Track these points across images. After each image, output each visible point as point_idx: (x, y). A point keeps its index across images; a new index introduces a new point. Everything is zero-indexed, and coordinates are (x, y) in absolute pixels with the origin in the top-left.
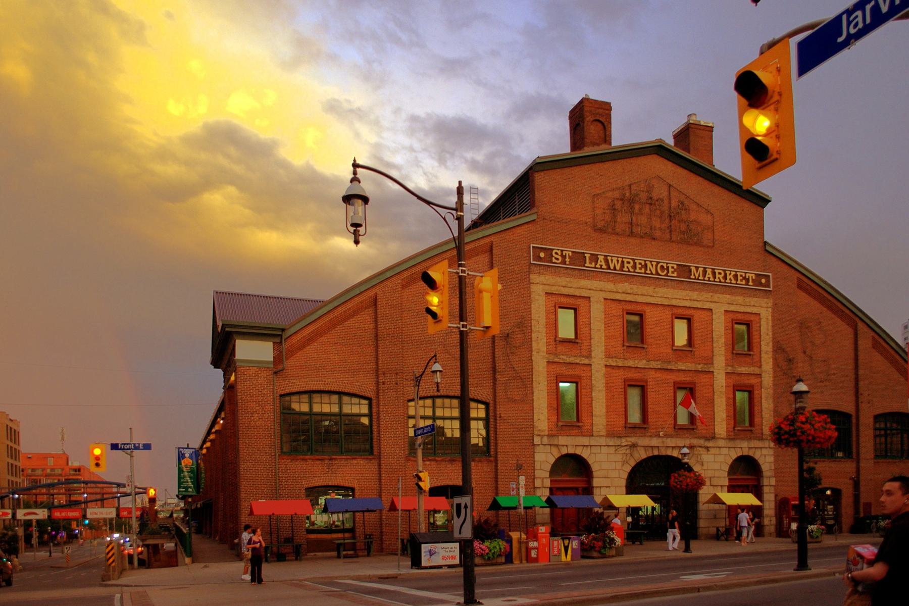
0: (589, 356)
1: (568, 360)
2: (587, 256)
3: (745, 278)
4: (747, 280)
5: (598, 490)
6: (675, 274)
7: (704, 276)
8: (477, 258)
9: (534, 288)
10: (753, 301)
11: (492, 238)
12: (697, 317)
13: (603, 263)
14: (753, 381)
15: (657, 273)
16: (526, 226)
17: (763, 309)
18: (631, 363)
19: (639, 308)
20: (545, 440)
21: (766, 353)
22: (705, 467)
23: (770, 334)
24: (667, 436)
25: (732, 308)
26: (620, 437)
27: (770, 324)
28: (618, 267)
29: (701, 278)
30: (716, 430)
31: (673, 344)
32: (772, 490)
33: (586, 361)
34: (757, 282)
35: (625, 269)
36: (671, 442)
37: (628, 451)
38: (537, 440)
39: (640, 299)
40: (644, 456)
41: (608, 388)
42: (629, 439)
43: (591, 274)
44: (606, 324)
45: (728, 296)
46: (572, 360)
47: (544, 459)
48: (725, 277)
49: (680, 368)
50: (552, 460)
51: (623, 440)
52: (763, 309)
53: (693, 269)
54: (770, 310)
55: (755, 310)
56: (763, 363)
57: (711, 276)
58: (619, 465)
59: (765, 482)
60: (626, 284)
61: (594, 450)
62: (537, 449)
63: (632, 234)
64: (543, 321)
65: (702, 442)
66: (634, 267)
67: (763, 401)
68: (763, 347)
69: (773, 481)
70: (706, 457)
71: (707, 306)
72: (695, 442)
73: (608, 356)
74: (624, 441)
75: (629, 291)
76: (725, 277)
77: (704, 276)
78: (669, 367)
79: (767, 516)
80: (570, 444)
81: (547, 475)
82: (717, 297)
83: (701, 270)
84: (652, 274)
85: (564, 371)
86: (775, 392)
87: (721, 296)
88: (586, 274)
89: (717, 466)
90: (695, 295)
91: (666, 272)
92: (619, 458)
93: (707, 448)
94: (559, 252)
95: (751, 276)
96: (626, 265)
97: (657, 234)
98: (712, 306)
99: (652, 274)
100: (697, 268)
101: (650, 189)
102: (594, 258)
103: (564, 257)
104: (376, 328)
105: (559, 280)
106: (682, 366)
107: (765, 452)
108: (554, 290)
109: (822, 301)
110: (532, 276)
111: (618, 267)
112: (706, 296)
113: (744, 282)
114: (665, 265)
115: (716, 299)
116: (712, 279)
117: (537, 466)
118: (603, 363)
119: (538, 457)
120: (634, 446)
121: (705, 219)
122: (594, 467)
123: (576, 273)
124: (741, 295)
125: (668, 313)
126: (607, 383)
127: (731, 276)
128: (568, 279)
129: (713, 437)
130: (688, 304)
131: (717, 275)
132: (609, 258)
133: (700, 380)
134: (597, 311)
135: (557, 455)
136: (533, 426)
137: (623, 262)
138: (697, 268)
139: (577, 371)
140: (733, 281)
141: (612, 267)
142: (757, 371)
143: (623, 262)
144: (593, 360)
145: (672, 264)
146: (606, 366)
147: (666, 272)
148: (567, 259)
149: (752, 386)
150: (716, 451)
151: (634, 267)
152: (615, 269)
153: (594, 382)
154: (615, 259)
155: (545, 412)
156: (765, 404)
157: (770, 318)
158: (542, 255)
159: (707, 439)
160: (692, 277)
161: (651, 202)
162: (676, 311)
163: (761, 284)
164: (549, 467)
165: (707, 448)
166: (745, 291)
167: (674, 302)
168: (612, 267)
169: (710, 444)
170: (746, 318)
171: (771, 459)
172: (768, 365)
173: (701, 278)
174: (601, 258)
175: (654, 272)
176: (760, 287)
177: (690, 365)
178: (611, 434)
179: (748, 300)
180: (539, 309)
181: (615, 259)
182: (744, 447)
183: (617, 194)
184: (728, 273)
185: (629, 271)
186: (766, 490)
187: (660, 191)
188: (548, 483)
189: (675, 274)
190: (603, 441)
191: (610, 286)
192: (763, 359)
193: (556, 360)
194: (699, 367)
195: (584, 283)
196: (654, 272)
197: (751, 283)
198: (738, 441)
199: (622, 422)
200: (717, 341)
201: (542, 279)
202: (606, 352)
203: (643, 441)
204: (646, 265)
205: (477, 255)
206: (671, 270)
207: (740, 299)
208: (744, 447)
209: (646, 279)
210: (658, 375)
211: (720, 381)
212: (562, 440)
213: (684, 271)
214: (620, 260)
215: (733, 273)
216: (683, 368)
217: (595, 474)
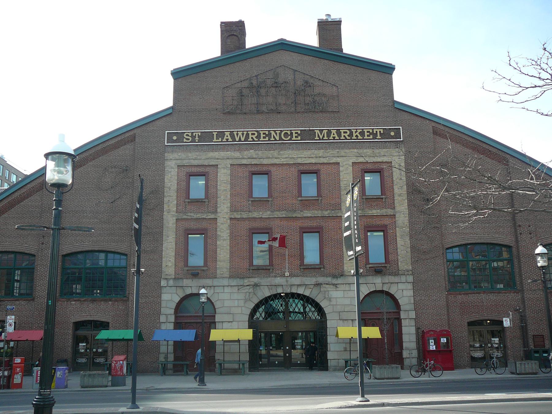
0: (216, 212)
1: (195, 216)
2: (215, 134)
3: (372, 133)
4: (375, 136)
5: (220, 324)
6: (299, 138)
7: (329, 136)
8: (125, 147)
9: (168, 163)
10: (383, 151)
11: (135, 131)
12: (324, 170)
13: (229, 137)
14: (387, 221)
15: (281, 139)
16: (164, 119)
17: (396, 158)
18: (255, 215)
19: (265, 169)
20: (171, 283)
21: (400, 195)
22: (334, 302)
24: (291, 275)
25: (361, 160)
26: (243, 278)
28: (243, 139)
29: (326, 138)
30: (345, 268)
31: (300, 194)
32: (413, 323)
33: (212, 216)
34: (385, 134)
35: (250, 139)
36: (296, 281)
37: (251, 290)
38: (163, 283)
39: (265, 162)
40: (268, 294)
41: (233, 237)
42: (252, 280)
43: (219, 147)
44: (231, 184)
45: (355, 150)
46: (199, 216)
47: (170, 298)
48: (351, 135)
49: (305, 215)
51: (246, 281)
52: (396, 158)
54: (403, 157)
55: (385, 159)
56: (397, 204)
57: (336, 135)
58: (242, 303)
60: (251, 151)
61: (218, 290)
62: (164, 290)
63: (259, 112)
64: (174, 187)
65: (329, 279)
66: (258, 137)
67: (398, 239)
68: (396, 190)
69: (413, 315)
70: (335, 294)
71: (334, 160)
72: (321, 280)
73: (233, 209)
74: (246, 282)
75: (254, 156)
76: (351, 135)
77: (329, 136)
78: (294, 215)
79: (407, 349)
80: (191, 286)
81: (172, 311)
82: (342, 152)
83: (325, 132)
84: (276, 140)
85: (193, 225)
86: (411, 229)
87: (347, 151)
88: (214, 148)
89: (347, 302)
90: (321, 153)
91: (289, 137)
92: (241, 296)
93: (335, 285)
94: (190, 134)
95: (379, 129)
96: (250, 136)
97: (283, 108)
98: (339, 160)
99: (276, 140)
100: (321, 131)
101: (277, 76)
102: (221, 135)
103: (193, 137)
105: (190, 155)
106: (308, 214)
107: (401, 286)
108: (185, 162)
109: (466, 144)
110: (166, 155)
111: (243, 139)
112: (331, 152)
113: (371, 137)
114: (289, 132)
115: (343, 154)
116: (337, 138)
117: (163, 304)
118: (227, 216)
119: (165, 297)
120: (256, 285)
121: (329, 90)
123: (205, 148)
124: (369, 148)
125: (294, 171)
126: (231, 233)
127: (357, 133)
128: (197, 154)
129: (342, 275)
130: (313, 161)
131: (343, 134)
132: (235, 133)
134: (223, 176)
135: (182, 295)
136: (161, 272)
137: (248, 135)
138: (321, 131)
139: (204, 225)
140: (360, 137)
141: (237, 139)
142: (390, 212)
143: (248, 134)
144: (219, 215)
146: (231, 219)
147: (289, 137)
148: (197, 138)
149: (386, 226)
150: (347, 287)
151: (258, 137)
152: (240, 140)
153: (219, 233)
154: (240, 133)
155: (173, 260)
156: (400, 242)
158: (175, 138)
159: (335, 276)
161: (276, 85)
162: (302, 168)
163: (392, 137)
164: (174, 306)
165: (335, 285)
166: (372, 145)
167: (299, 161)
168: (237, 139)
169: (340, 281)
170: (376, 166)
171: (411, 293)
172: (402, 207)
173: (326, 138)
174: (227, 134)
175: (278, 139)
176: (389, 137)
177: (316, 212)
178: (231, 277)
180: (171, 179)
181: (240, 133)
182: (377, 283)
183: (246, 84)
184: (354, 131)
185: (254, 141)
187: (286, 76)
188: (172, 319)
189: (299, 138)
190: (225, 282)
191: (237, 154)
192: (396, 202)
193: (186, 217)
194: (326, 213)
195: (211, 154)
196: (278, 139)
197: (379, 137)
198: (370, 277)
199: (246, 264)
201: (175, 155)
202: (231, 206)
203: (265, 281)
204: (269, 135)
205: (125, 144)
206: (294, 135)
207: (369, 151)
208: (377, 283)
209: (270, 146)
210: (284, 223)
212: (186, 282)
213: (309, 135)
214: (245, 133)
215: (359, 131)
216: (309, 215)
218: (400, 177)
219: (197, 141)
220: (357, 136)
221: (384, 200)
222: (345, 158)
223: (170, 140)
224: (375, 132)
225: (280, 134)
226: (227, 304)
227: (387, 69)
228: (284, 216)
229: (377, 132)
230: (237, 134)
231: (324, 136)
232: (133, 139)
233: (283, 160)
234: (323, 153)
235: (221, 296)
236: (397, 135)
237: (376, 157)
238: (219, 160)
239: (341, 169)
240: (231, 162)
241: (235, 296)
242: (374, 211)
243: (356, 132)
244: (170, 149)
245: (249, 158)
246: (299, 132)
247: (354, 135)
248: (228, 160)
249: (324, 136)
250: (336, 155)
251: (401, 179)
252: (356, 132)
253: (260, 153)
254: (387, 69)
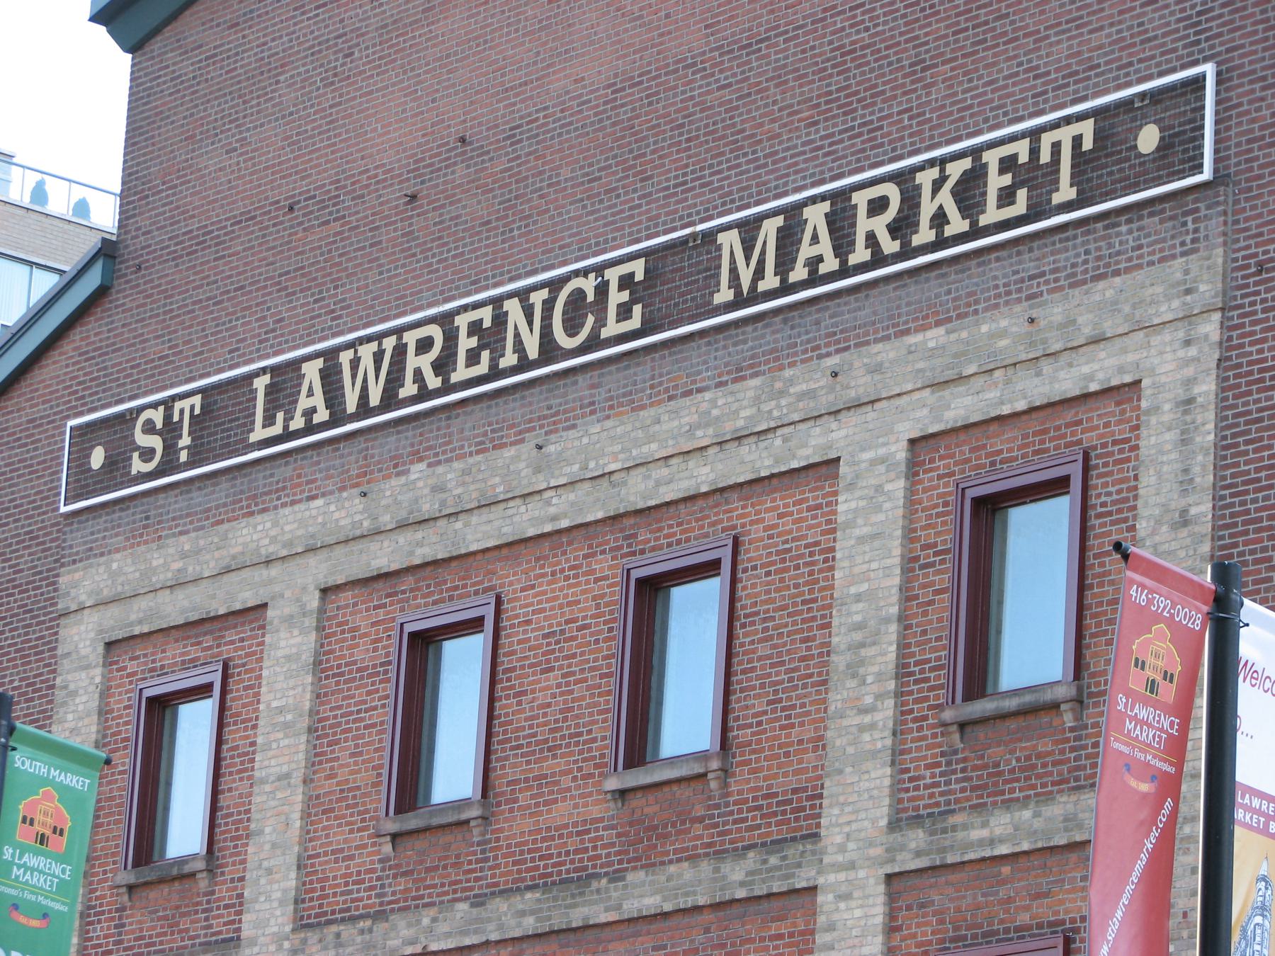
23: (1202, 508)
25: (963, 406)
27: (1207, 436)
34: (1101, 164)
39: (477, 533)
45: (935, 337)
49: (632, 906)
53: (729, 240)
54: (1211, 328)
71: (809, 447)
75: (428, 507)
78: (577, 917)
82: (858, 372)
103: (170, 430)
114: (588, 285)
115: (860, 384)
127: (945, 198)
128: (186, 543)
130: (702, 475)
138: (749, 229)
157: (1207, 388)
160: (725, 295)
177: (685, 872)
179: (1054, 311)
197: (1066, 192)
200: (853, 670)
207: (1002, 329)
215: (956, 170)
216: (652, 904)
218: (1178, 503)
219: (183, 456)
220: (940, 219)
221: (1068, 719)
222: (870, 414)
224: (1045, 157)
225: (549, 305)
228: (530, 924)
229: (1056, 147)
230: (355, 363)
231: (759, 274)
233: (559, 503)
234: (757, 401)
237: (1047, 367)
238: (274, 571)
239: (845, 505)
240: (320, 570)
242: (1001, 823)
243: (937, 186)
244: (77, 539)
245: (402, 526)
246: (638, 268)
247: (927, 210)
248: (312, 560)
249: (759, 274)
250: (825, 402)
251: (1184, 520)
252: (937, 186)
253: (450, 474)
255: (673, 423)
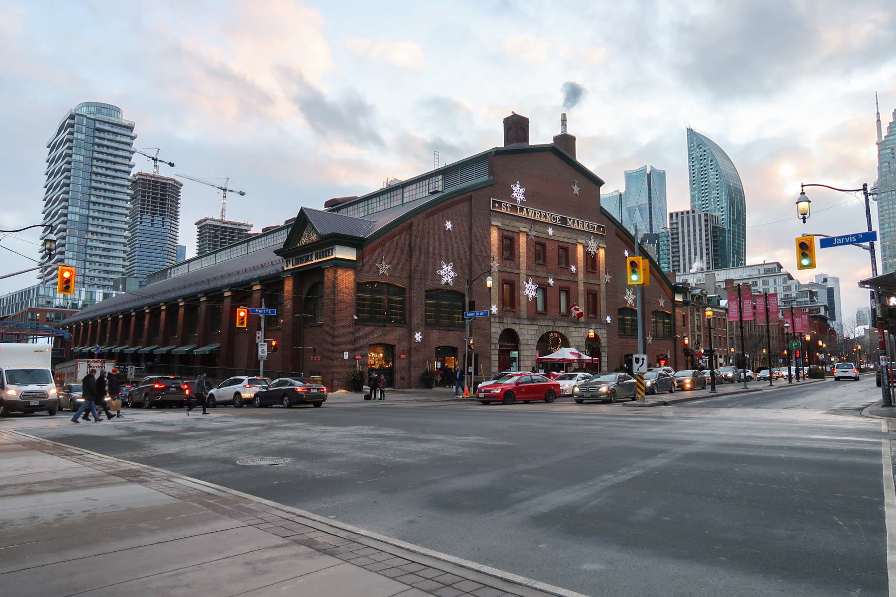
0: (519, 268)
1: (509, 270)
19: (543, 241)
20: (497, 320)
47: (496, 330)
50: (500, 332)
59: (602, 350)
61: (522, 326)
73: (528, 268)
89: (580, 339)
90: (569, 235)
95: (596, 226)
104: (411, 243)
112: (575, 236)
119: (493, 330)
122: (521, 338)
130: (565, 240)
133: (572, 286)
145: (559, 216)
167: (559, 239)
171: (605, 336)
178: (528, 318)
186: (603, 354)
190: (526, 322)
211: (581, 287)
217: (521, 342)
223: (494, 206)
226: (526, 337)
227: (599, 183)
232: (470, 199)
235: (525, 332)
236: (603, 232)
241: (530, 332)
254: (599, 183)
255: (563, 234)
